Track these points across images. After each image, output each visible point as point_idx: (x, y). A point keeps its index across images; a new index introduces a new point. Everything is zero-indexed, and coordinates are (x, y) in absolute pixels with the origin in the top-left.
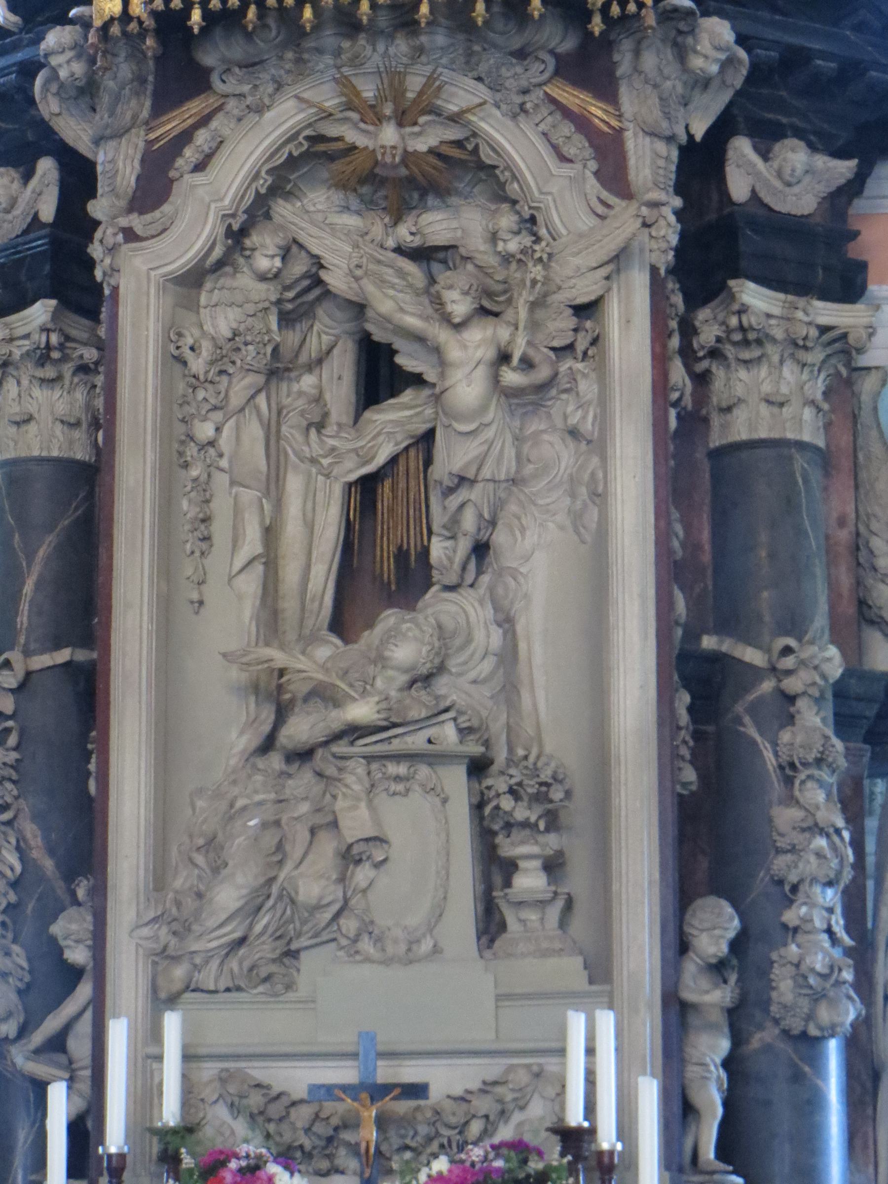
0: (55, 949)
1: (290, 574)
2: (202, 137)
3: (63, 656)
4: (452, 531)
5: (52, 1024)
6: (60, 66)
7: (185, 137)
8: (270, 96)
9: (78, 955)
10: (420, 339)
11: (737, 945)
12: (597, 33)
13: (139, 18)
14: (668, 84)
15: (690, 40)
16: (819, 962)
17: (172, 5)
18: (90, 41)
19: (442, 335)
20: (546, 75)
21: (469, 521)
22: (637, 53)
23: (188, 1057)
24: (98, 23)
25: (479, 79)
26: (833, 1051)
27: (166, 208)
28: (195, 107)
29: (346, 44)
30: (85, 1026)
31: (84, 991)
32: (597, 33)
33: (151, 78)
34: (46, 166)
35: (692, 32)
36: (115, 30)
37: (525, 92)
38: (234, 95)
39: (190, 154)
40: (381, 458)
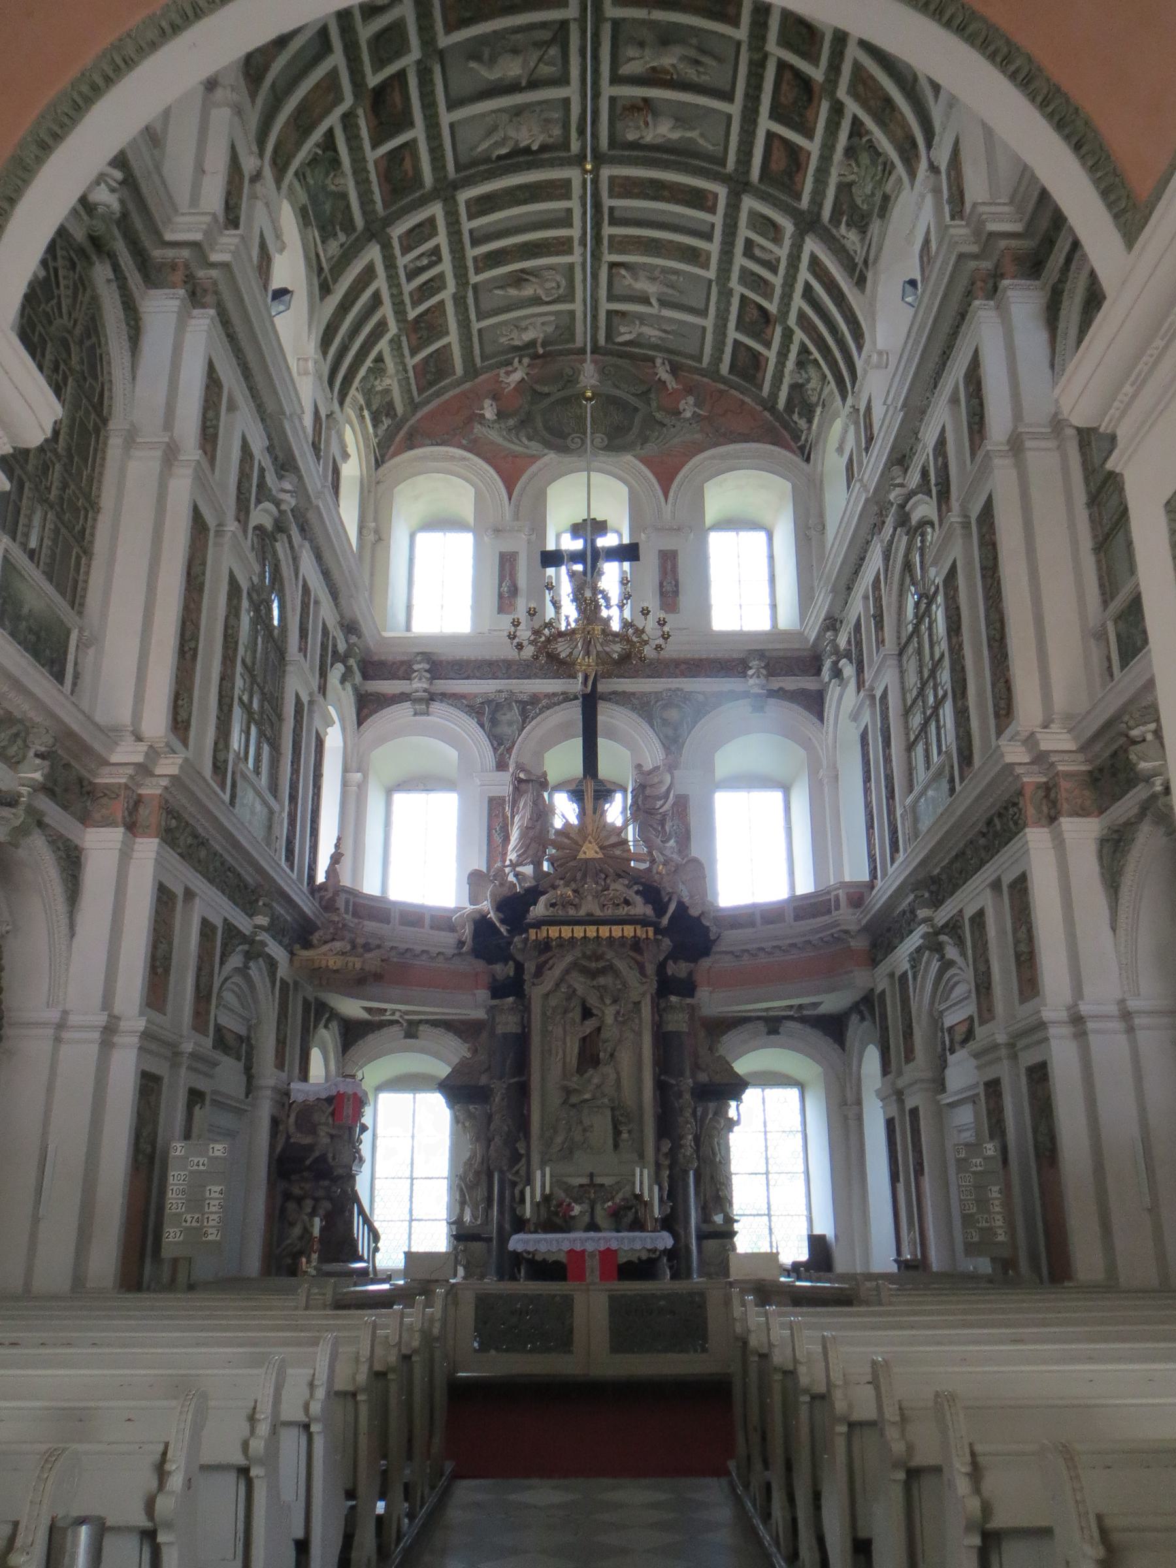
0: (516, 1150)
1: (568, 1060)
2: (551, 962)
3: (515, 1080)
4: (605, 1051)
5: (515, 1169)
7: (546, 962)
9: (522, 1151)
11: (671, 1149)
16: (688, 1153)
23: (551, 1176)
26: (691, 1173)
28: (549, 954)
30: (524, 1168)
31: (524, 1160)
34: (511, 963)
39: (548, 966)
40: (588, 1031)
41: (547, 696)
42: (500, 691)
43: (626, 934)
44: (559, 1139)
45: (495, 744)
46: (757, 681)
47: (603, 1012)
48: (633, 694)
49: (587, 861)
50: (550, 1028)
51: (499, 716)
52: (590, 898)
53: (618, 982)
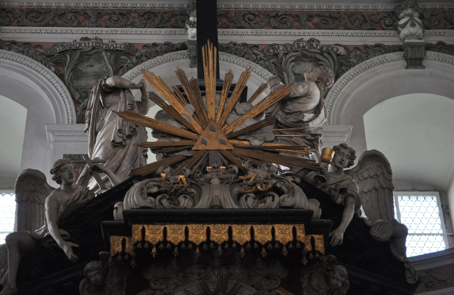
6: (92, 276)
8: (173, 290)
12: (305, 264)
13: (128, 254)
14: (321, 291)
15: (331, 273)
17: (145, 246)
18: (109, 261)
20: (278, 285)
22: (310, 279)
24: (112, 255)
25: (253, 286)
29: (203, 271)
32: (305, 264)
33: (125, 284)
35: (332, 270)
36: (119, 257)
37: (270, 291)
38: (159, 289)
41: (145, 46)
42: (86, 39)
43: (279, 237)
45: (77, 97)
46: (413, 30)
48: (256, 46)
49: (207, 154)
51: (84, 68)
52: (215, 181)
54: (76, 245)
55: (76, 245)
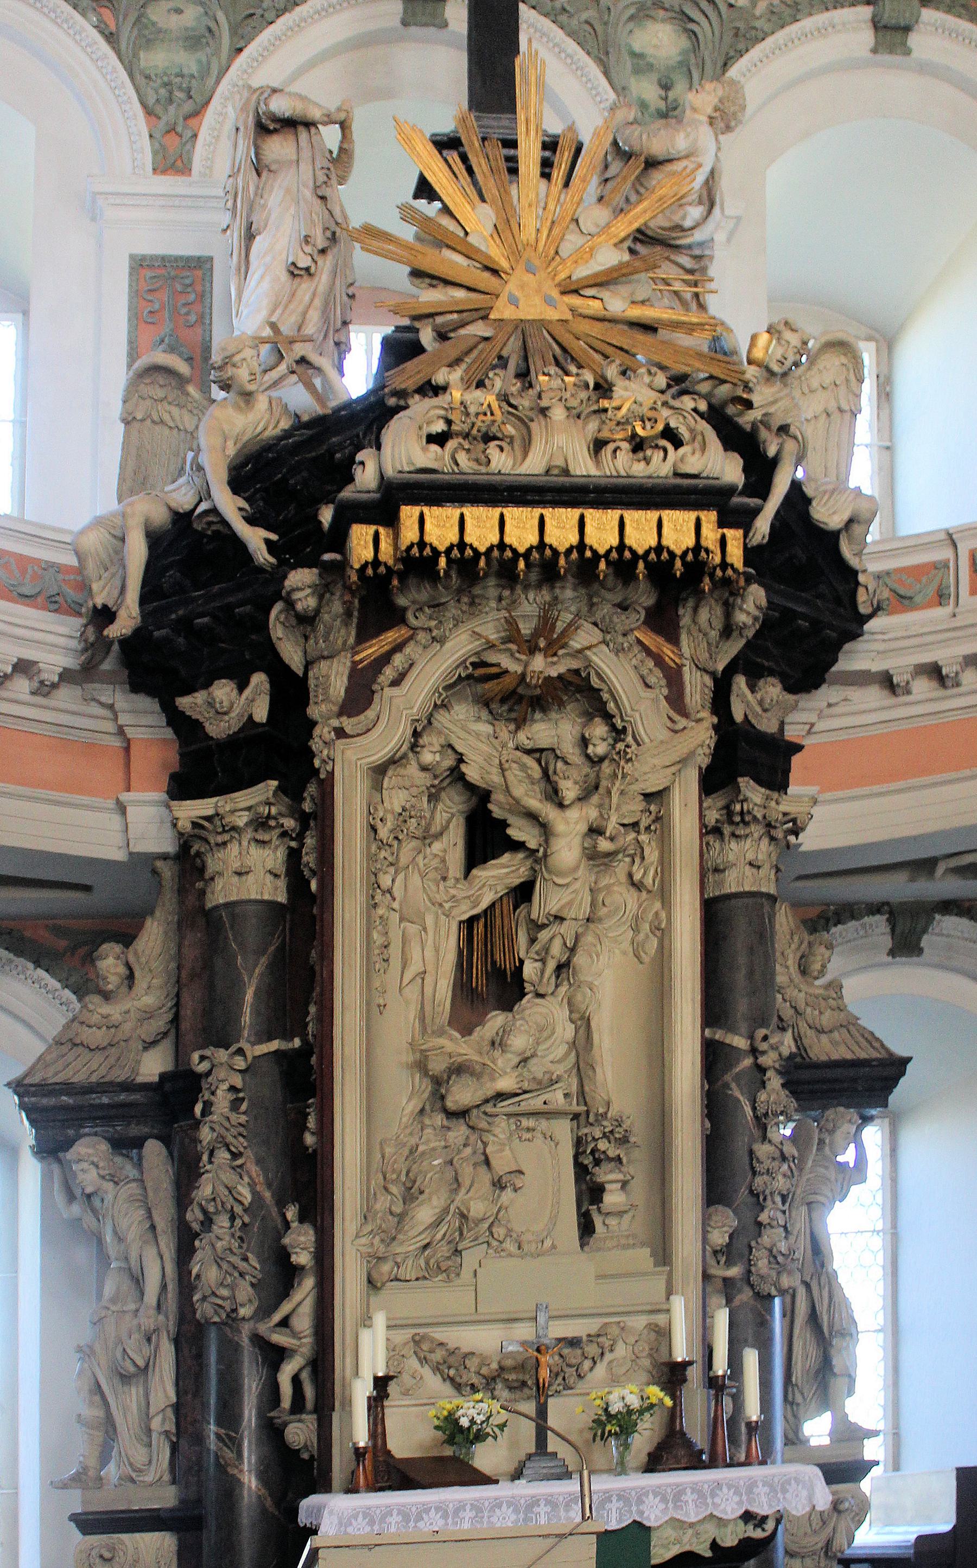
7: (386, 659)
10: (532, 816)
19: (548, 812)
21: (556, 949)
27: (370, 714)
28: (391, 636)
39: (389, 673)
44: (424, 1214)
47: (545, 829)
50: (385, 881)
53: (599, 730)
54: (274, 537)
55: (274, 537)
